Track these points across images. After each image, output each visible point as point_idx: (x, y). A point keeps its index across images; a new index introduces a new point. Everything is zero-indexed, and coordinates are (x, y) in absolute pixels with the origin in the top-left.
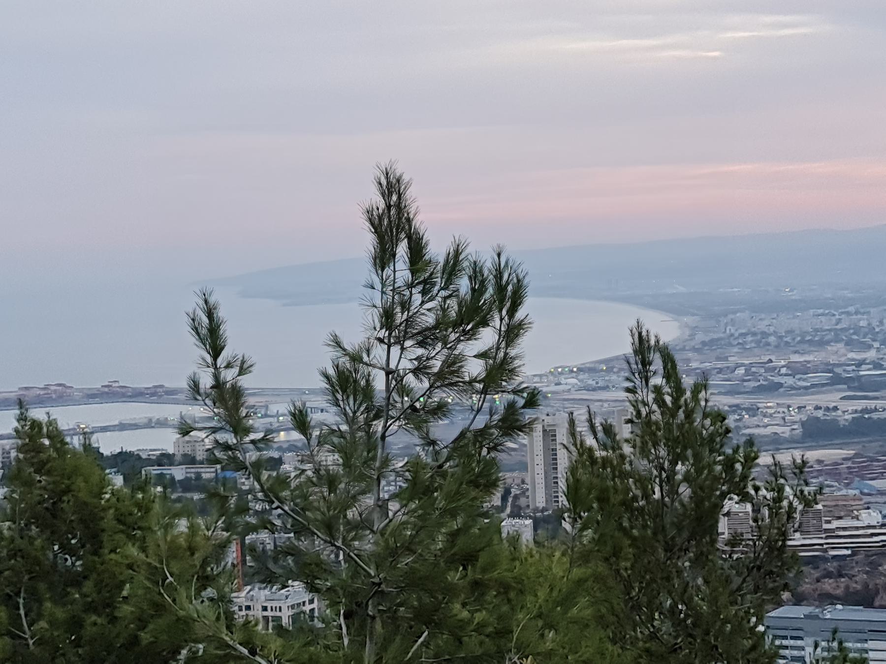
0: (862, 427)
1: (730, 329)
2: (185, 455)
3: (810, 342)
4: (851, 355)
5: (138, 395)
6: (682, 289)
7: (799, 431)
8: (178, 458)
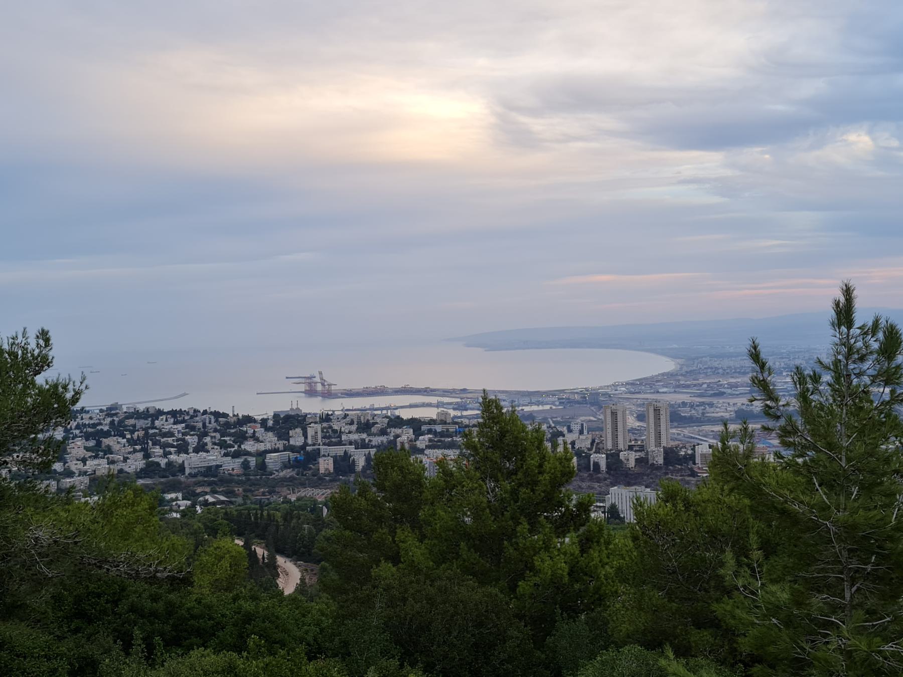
1: (700, 365)
2: (442, 420)
3: (739, 373)
5: (417, 392)
6: (675, 346)
7: (733, 415)
8: (438, 421)
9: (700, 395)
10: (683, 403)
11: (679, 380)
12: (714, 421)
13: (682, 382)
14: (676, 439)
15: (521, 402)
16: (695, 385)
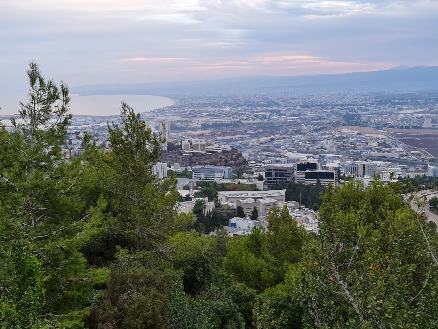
0: (215, 125)
1: (186, 103)
3: (204, 106)
4: (213, 109)
6: (174, 93)
9: (186, 117)
10: (178, 121)
11: (176, 110)
12: (192, 129)
13: (177, 111)
14: (174, 138)
15: (99, 121)
16: (183, 112)
